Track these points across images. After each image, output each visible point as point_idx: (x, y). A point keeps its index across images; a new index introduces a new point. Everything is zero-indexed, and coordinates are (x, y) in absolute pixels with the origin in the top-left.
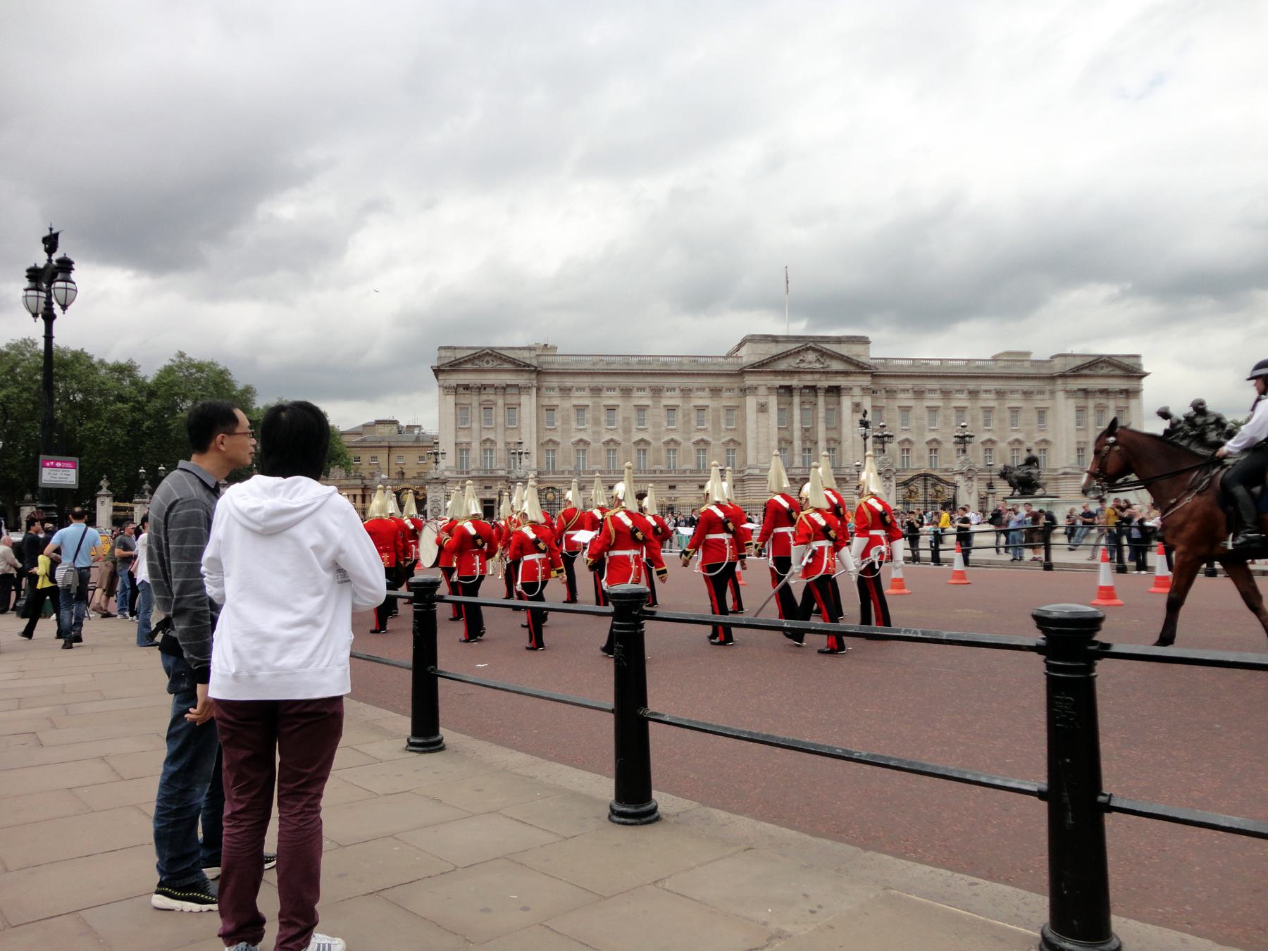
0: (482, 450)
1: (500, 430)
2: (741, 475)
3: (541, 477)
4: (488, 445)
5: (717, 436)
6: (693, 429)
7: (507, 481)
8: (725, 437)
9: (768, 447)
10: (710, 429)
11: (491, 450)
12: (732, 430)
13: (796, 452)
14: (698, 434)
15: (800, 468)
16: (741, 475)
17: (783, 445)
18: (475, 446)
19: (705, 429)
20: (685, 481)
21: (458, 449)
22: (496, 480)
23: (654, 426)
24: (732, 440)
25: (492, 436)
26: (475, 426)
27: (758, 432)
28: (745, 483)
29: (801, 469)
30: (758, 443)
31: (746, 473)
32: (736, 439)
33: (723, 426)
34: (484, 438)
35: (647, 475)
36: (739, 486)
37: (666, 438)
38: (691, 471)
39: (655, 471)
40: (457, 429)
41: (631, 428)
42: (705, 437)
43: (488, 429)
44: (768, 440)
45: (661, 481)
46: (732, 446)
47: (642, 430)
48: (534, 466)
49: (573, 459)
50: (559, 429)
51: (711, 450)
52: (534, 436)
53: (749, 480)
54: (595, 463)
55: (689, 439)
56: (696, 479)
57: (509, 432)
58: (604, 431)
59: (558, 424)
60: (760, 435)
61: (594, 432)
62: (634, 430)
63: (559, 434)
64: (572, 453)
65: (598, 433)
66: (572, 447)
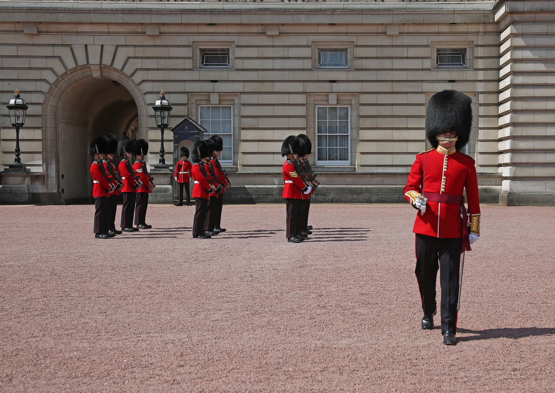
36: (480, 52)
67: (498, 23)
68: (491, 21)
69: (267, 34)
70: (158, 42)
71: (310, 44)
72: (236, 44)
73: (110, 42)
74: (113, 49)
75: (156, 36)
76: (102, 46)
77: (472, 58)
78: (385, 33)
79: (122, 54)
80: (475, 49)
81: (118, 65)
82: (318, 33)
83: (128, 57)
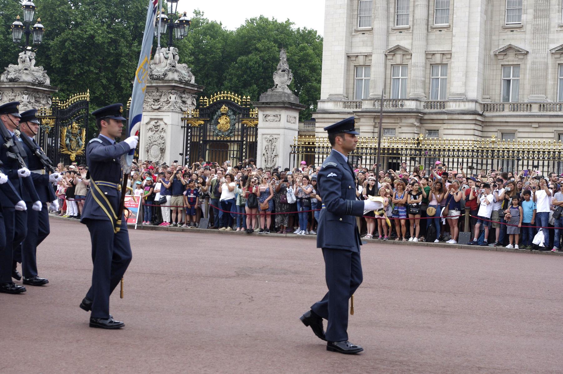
0: (389, 67)
1: (420, 30)
3: (486, 114)
4: (398, 59)
7: (422, 121)
11: (404, 66)
18: (377, 60)
21: (352, 65)
22: (400, 118)
25: (404, 42)
26: (379, 25)
34: (392, 45)
40: (353, 33)
43: (401, 31)
48: (473, 94)
49: (550, 82)
50: (529, 28)
52: (476, 39)
57: (434, 35)
59: (527, 17)
63: (528, 36)
64: (550, 71)
66: (550, 61)
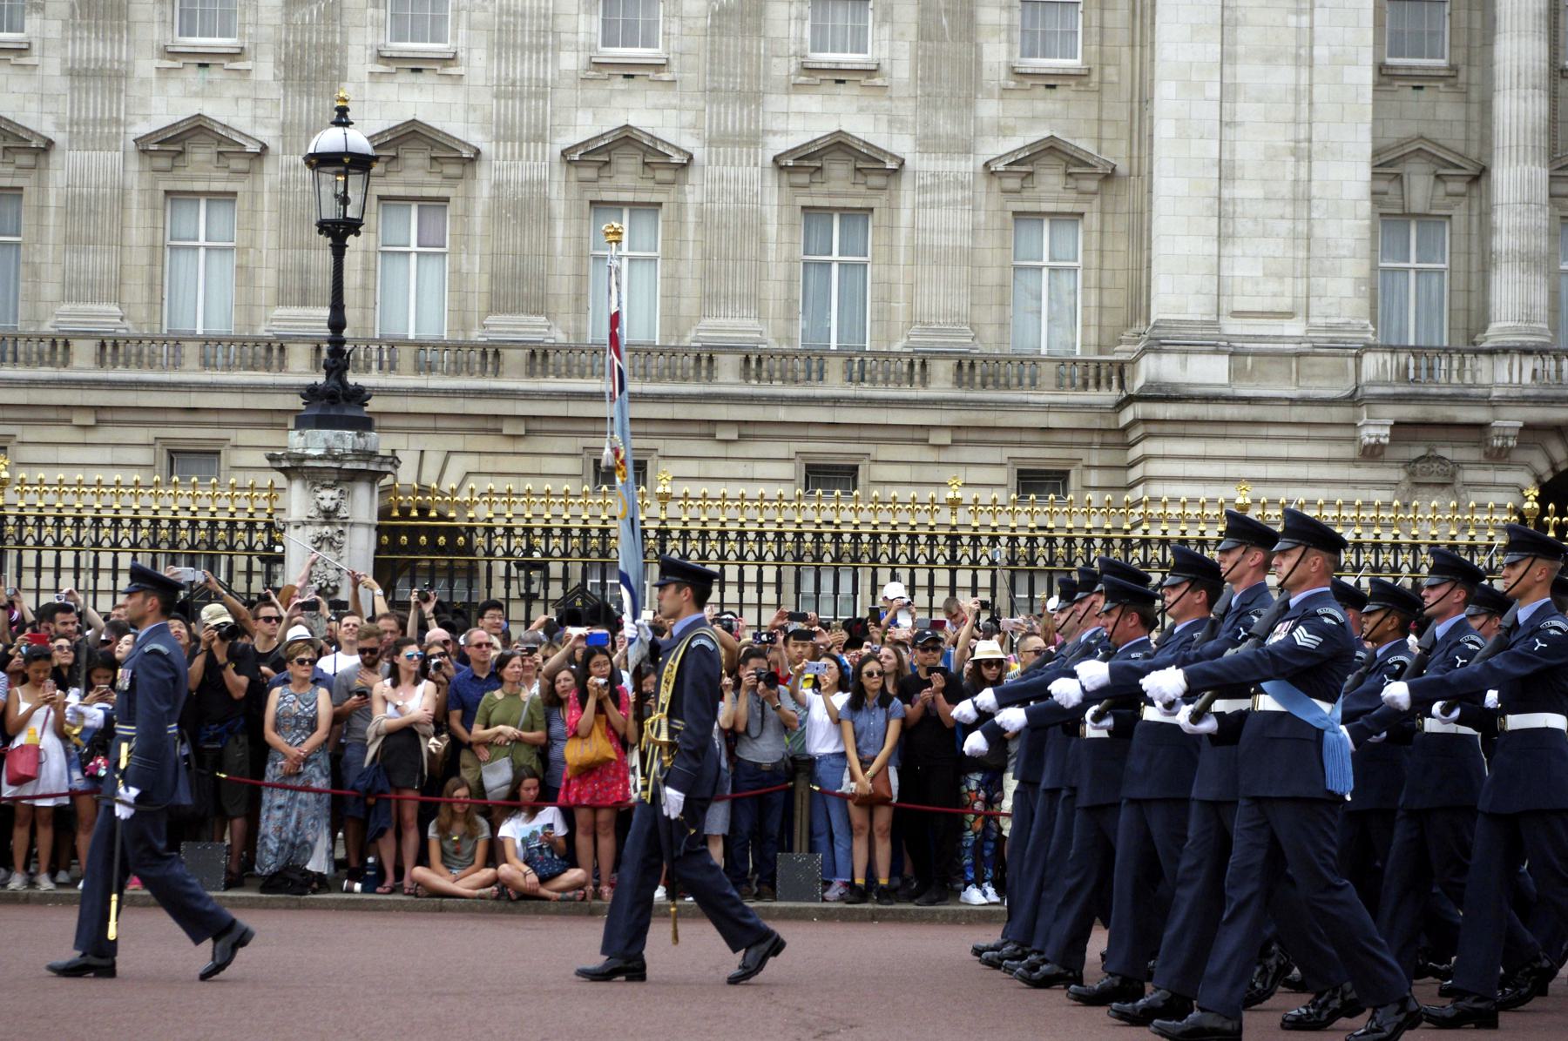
2: (1109, 396)
5: (944, 125)
6: (782, 68)
8: (1002, 131)
9: (1302, 198)
10: (902, 71)
12: (1051, 82)
13: (1503, 242)
14: (810, 102)
15: (1526, 351)
16: (1109, 396)
17: (1420, 189)
19: (870, 73)
20: (707, 429)
23: (504, 43)
24: (1050, 149)
27: (1228, 93)
28: (1136, 452)
29: (1530, 364)
30: (1226, 172)
31: (1137, 384)
32: (1085, 145)
33: (996, 54)
35: (435, 382)
36: (1094, 478)
37: (585, 126)
38: (753, 361)
39: (491, 356)
41: (343, 48)
42: (864, 128)
44: (1303, 152)
45: (534, 426)
46: (1050, 189)
47: (417, 66)
51: (905, 217)
53: (1154, 428)
54: (74, 289)
55: (753, 139)
56: (782, 414)
58: (146, 65)
60: (1245, 110)
61: (78, 74)
62: (359, 64)
65: (113, 77)
67: (1125, 430)
68: (1113, 427)
69: (718, 437)
70: (522, 446)
71: (793, 456)
72: (661, 452)
73: (436, 445)
74: (440, 458)
75: (519, 436)
76: (422, 452)
77: (1079, 487)
78: (927, 440)
79: (458, 466)
80: (1086, 472)
81: (450, 483)
82: (807, 437)
83: (468, 473)
